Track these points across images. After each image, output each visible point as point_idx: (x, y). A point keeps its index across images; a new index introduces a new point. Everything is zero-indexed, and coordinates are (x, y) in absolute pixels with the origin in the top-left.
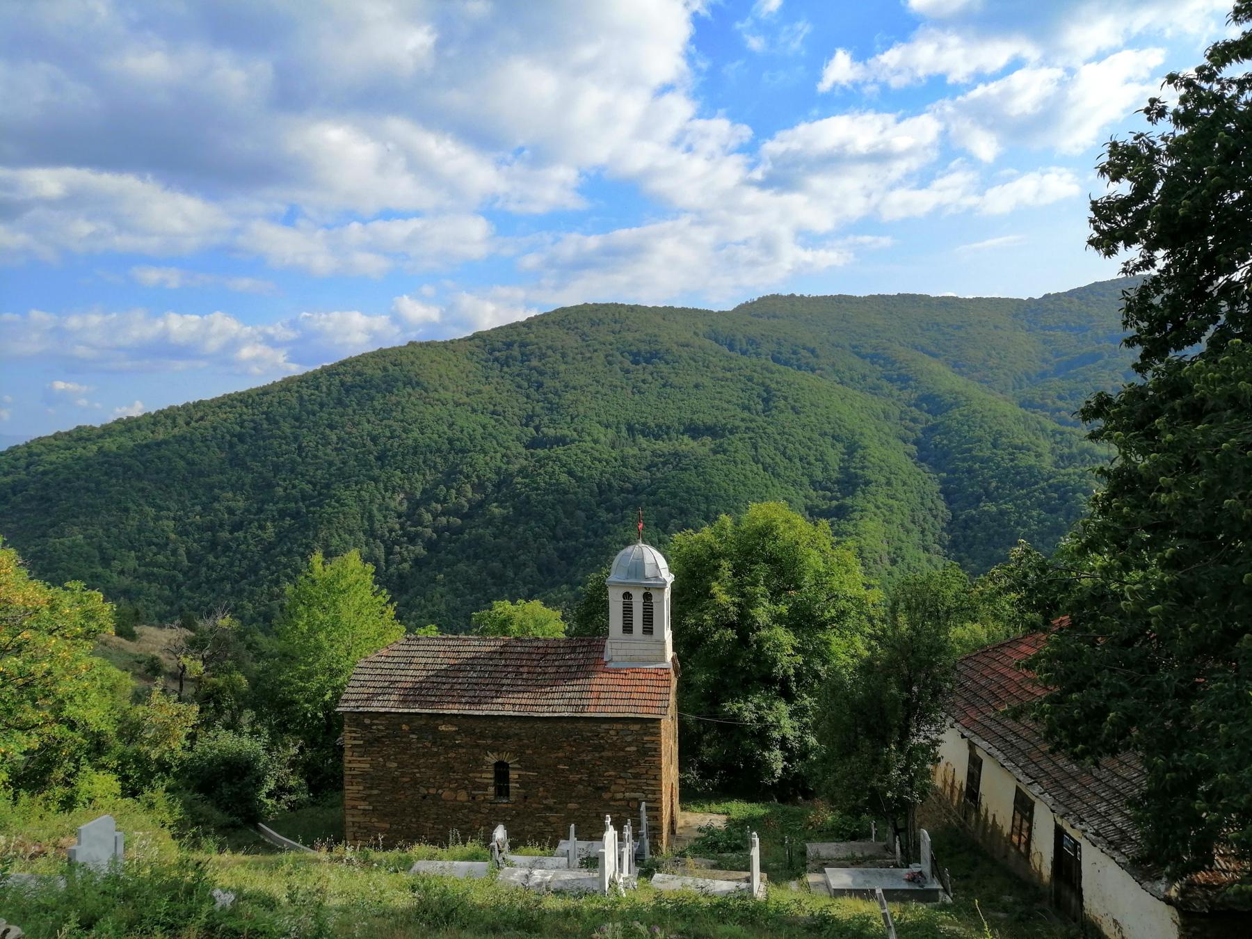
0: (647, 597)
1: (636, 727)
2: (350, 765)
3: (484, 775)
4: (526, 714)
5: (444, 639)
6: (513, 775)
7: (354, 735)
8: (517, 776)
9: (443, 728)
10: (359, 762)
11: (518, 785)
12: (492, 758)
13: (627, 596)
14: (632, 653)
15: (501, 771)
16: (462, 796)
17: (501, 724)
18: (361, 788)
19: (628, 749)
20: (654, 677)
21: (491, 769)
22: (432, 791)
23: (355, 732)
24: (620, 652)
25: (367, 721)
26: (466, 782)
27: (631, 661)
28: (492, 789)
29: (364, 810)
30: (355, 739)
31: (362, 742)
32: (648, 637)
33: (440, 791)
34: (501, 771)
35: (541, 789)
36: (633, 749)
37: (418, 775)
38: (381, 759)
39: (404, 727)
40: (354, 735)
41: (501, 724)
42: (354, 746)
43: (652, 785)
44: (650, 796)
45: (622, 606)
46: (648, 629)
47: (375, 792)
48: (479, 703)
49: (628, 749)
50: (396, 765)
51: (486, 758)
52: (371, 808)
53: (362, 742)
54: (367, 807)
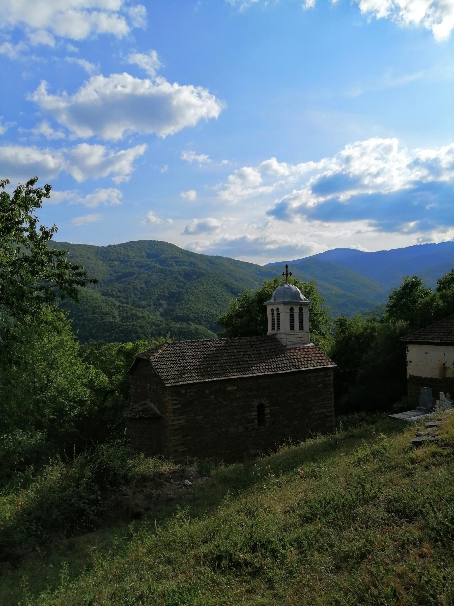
0: (301, 310)
1: (322, 374)
2: (173, 423)
3: (253, 414)
4: (275, 373)
5: (190, 342)
6: (267, 411)
7: (175, 402)
8: (269, 411)
9: (229, 388)
10: (179, 420)
11: (270, 416)
12: (256, 403)
13: (292, 309)
14: (295, 340)
15: (261, 408)
16: (241, 429)
17: (260, 381)
18: (180, 437)
19: (319, 386)
20: (311, 350)
21: (256, 409)
22: (224, 430)
23: (175, 400)
24: (291, 340)
25: (183, 391)
26: (243, 420)
27: (295, 344)
28: (256, 421)
29: (183, 451)
30: (176, 404)
31: (180, 406)
32: (301, 331)
33: (229, 429)
34: (261, 408)
35: (281, 416)
36: (321, 385)
37: (216, 421)
38: (192, 415)
39: (207, 391)
40: (175, 402)
41: (260, 381)
42: (175, 409)
43: (330, 403)
44: (329, 409)
45: (289, 314)
46: (301, 327)
47: (189, 438)
48: (245, 371)
49: (319, 386)
50: (202, 417)
51: (254, 403)
52: (187, 449)
53: (180, 406)
54: (184, 449)
